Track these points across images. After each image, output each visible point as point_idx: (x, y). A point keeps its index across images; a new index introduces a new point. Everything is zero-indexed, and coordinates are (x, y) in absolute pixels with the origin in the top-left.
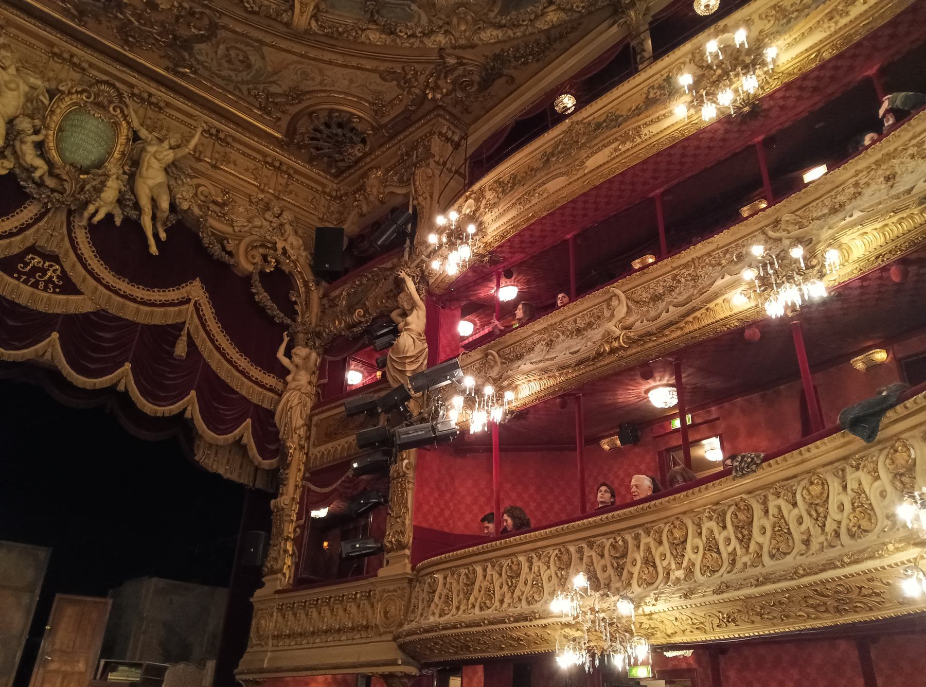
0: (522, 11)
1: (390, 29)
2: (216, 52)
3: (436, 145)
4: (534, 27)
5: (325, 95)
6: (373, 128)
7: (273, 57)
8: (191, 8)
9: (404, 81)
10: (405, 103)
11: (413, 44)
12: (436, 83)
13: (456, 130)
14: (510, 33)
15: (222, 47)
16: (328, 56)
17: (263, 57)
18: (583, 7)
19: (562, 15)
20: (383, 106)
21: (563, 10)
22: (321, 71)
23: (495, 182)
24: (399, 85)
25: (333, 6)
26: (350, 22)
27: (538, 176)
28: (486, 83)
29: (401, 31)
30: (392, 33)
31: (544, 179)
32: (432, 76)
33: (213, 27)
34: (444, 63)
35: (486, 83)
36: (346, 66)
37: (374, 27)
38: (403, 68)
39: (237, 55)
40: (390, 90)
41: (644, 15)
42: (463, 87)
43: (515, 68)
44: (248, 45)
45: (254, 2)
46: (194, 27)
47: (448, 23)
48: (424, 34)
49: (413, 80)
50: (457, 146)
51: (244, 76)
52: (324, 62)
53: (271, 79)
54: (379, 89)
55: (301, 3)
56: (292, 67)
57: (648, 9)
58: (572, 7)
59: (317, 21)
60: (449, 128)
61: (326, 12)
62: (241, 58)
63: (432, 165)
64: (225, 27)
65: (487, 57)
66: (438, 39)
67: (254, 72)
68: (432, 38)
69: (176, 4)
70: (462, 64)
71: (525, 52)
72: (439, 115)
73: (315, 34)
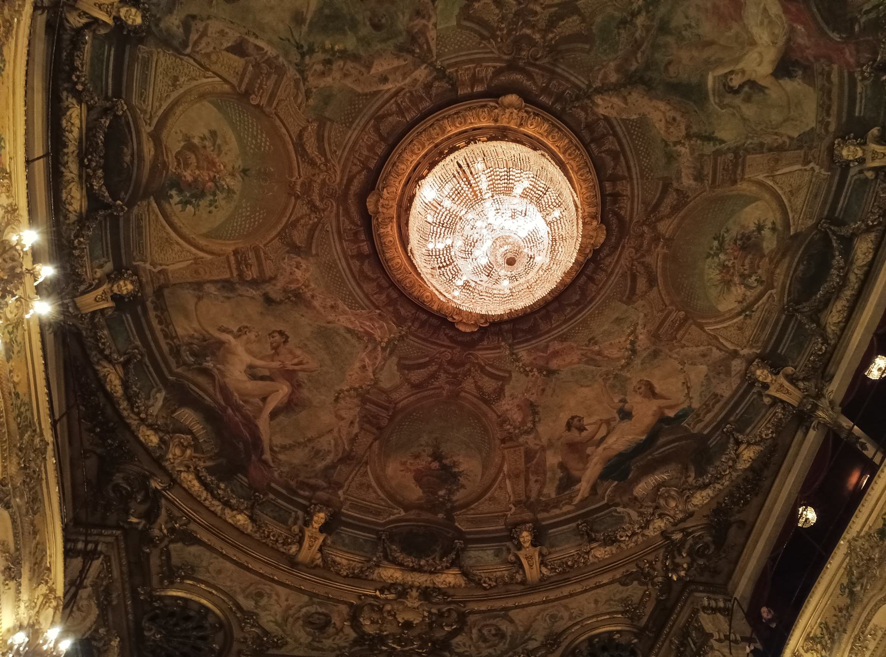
0: (718, 463)
1: (611, 539)
2: (471, 639)
3: (707, 621)
4: (736, 470)
5: (578, 627)
6: (636, 635)
7: (519, 616)
8: (439, 610)
9: (642, 576)
10: (654, 595)
11: (636, 541)
12: (673, 562)
13: (717, 597)
14: (718, 486)
15: (474, 631)
16: (566, 591)
17: (512, 621)
18: (772, 433)
19: (758, 448)
20: (636, 609)
21: (756, 443)
22: (566, 607)
23: (806, 640)
24: (642, 584)
25: (552, 546)
26: (573, 551)
27: (855, 614)
28: (720, 540)
29: (621, 537)
30: (613, 542)
31: (865, 615)
32: (667, 559)
33: (462, 617)
34: (672, 541)
35: (720, 540)
36: (586, 591)
37: (595, 545)
38: (637, 565)
39: (490, 631)
40: (635, 591)
41: (832, 409)
42: (700, 554)
43: (739, 512)
44: (495, 617)
45: (490, 579)
46: (447, 625)
47: (657, 508)
48: (641, 527)
49: (651, 571)
50: (728, 612)
51: (502, 646)
52: (566, 597)
53: (526, 637)
54: (625, 595)
55: (527, 558)
56: (539, 617)
57: (831, 403)
58: (761, 437)
59: (546, 566)
60: (709, 598)
61: (550, 553)
62: (493, 632)
63: (716, 645)
64: (472, 612)
65: (707, 516)
66: (656, 525)
67: (509, 639)
68: (651, 527)
69: (426, 614)
70: (689, 534)
71: (740, 494)
72: (692, 591)
73: (549, 577)
